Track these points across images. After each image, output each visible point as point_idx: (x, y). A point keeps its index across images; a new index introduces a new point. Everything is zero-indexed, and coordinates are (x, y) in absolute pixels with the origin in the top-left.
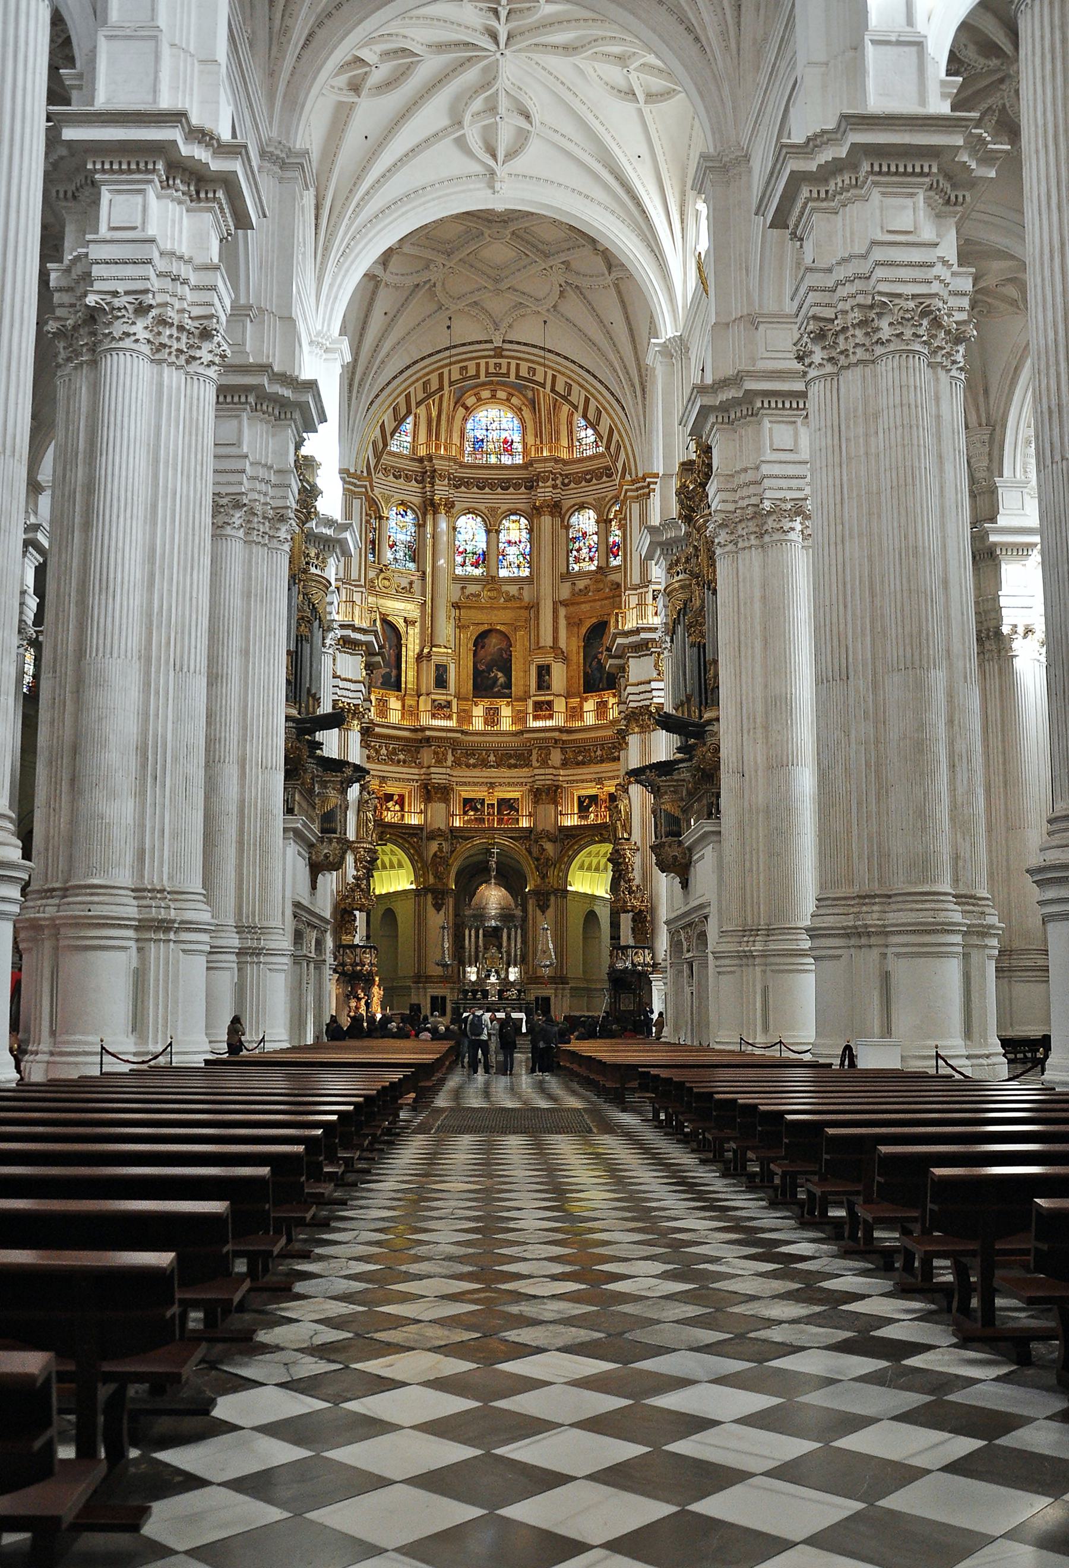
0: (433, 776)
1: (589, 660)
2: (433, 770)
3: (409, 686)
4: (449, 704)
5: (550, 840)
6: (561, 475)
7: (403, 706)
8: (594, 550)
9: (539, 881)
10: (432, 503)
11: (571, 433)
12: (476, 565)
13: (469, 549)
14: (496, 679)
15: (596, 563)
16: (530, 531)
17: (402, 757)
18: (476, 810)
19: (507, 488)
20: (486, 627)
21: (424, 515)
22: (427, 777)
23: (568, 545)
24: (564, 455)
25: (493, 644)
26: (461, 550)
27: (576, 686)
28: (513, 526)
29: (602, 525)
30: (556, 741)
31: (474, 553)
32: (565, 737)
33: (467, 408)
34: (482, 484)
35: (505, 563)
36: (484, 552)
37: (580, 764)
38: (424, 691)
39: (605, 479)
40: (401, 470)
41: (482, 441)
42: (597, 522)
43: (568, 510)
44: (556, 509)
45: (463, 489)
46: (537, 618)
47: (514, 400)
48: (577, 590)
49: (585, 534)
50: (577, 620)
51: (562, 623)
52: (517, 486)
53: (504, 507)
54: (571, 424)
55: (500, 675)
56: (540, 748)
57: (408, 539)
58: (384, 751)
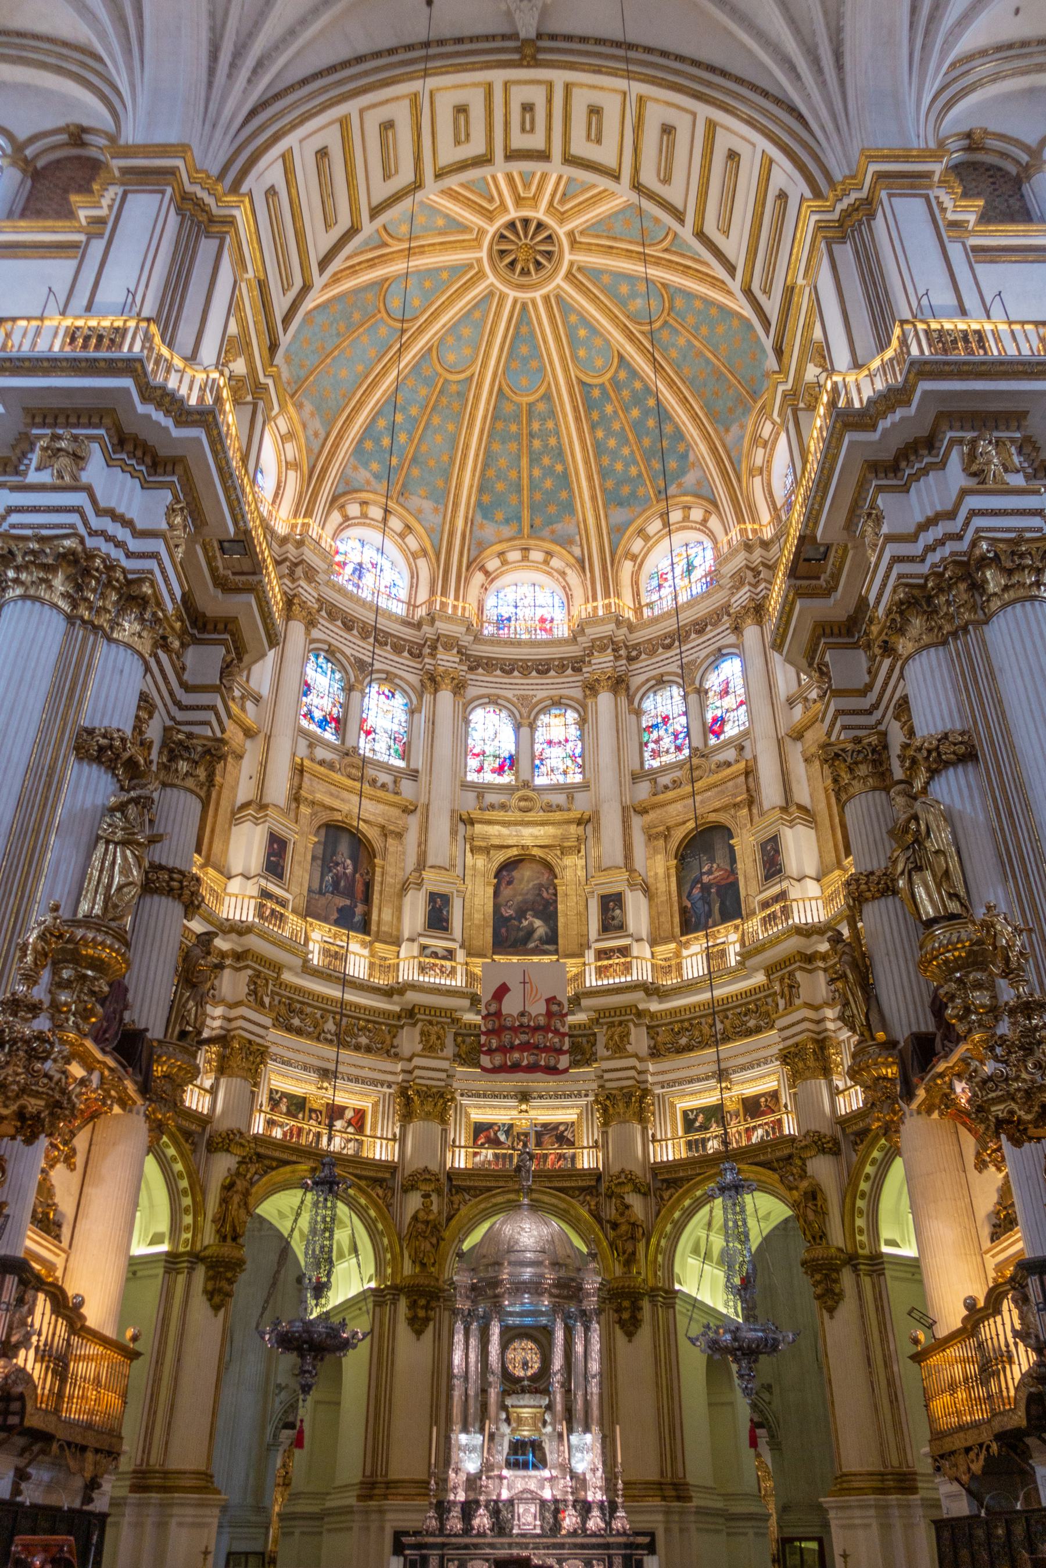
0: (417, 1073)
1: (687, 888)
2: (417, 1061)
3: (384, 928)
4: (450, 955)
5: (637, 1190)
6: (626, 647)
7: (372, 955)
8: (682, 736)
9: (619, 1270)
10: (433, 679)
11: (637, 594)
12: (500, 770)
13: (489, 750)
14: (531, 932)
15: (686, 752)
16: (582, 722)
17: (363, 1040)
18: (496, 1143)
19: (548, 671)
20: (514, 852)
21: (420, 697)
22: (407, 1077)
23: (640, 737)
24: (629, 615)
25: (527, 878)
26: (475, 751)
27: (667, 926)
28: (554, 721)
29: (693, 698)
30: (640, 1014)
31: (496, 757)
32: (655, 1006)
33: (487, 573)
34: (508, 668)
35: (543, 769)
36: (511, 757)
37: (681, 1050)
38: (406, 935)
39: (693, 636)
40: (387, 634)
41: (509, 619)
42: (685, 697)
43: (638, 689)
44: (619, 684)
45: (480, 670)
46: (597, 830)
47: (555, 562)
48: (660, 788)
49: (666, 719)
50: (661, 828)
51: (638, 839)
52: (562, 668)
53: (541, 695)
54: (637, 584)
55: (538, 923)
56: (611, 1025)
57: (396, 728)
58: (330, 1026)
